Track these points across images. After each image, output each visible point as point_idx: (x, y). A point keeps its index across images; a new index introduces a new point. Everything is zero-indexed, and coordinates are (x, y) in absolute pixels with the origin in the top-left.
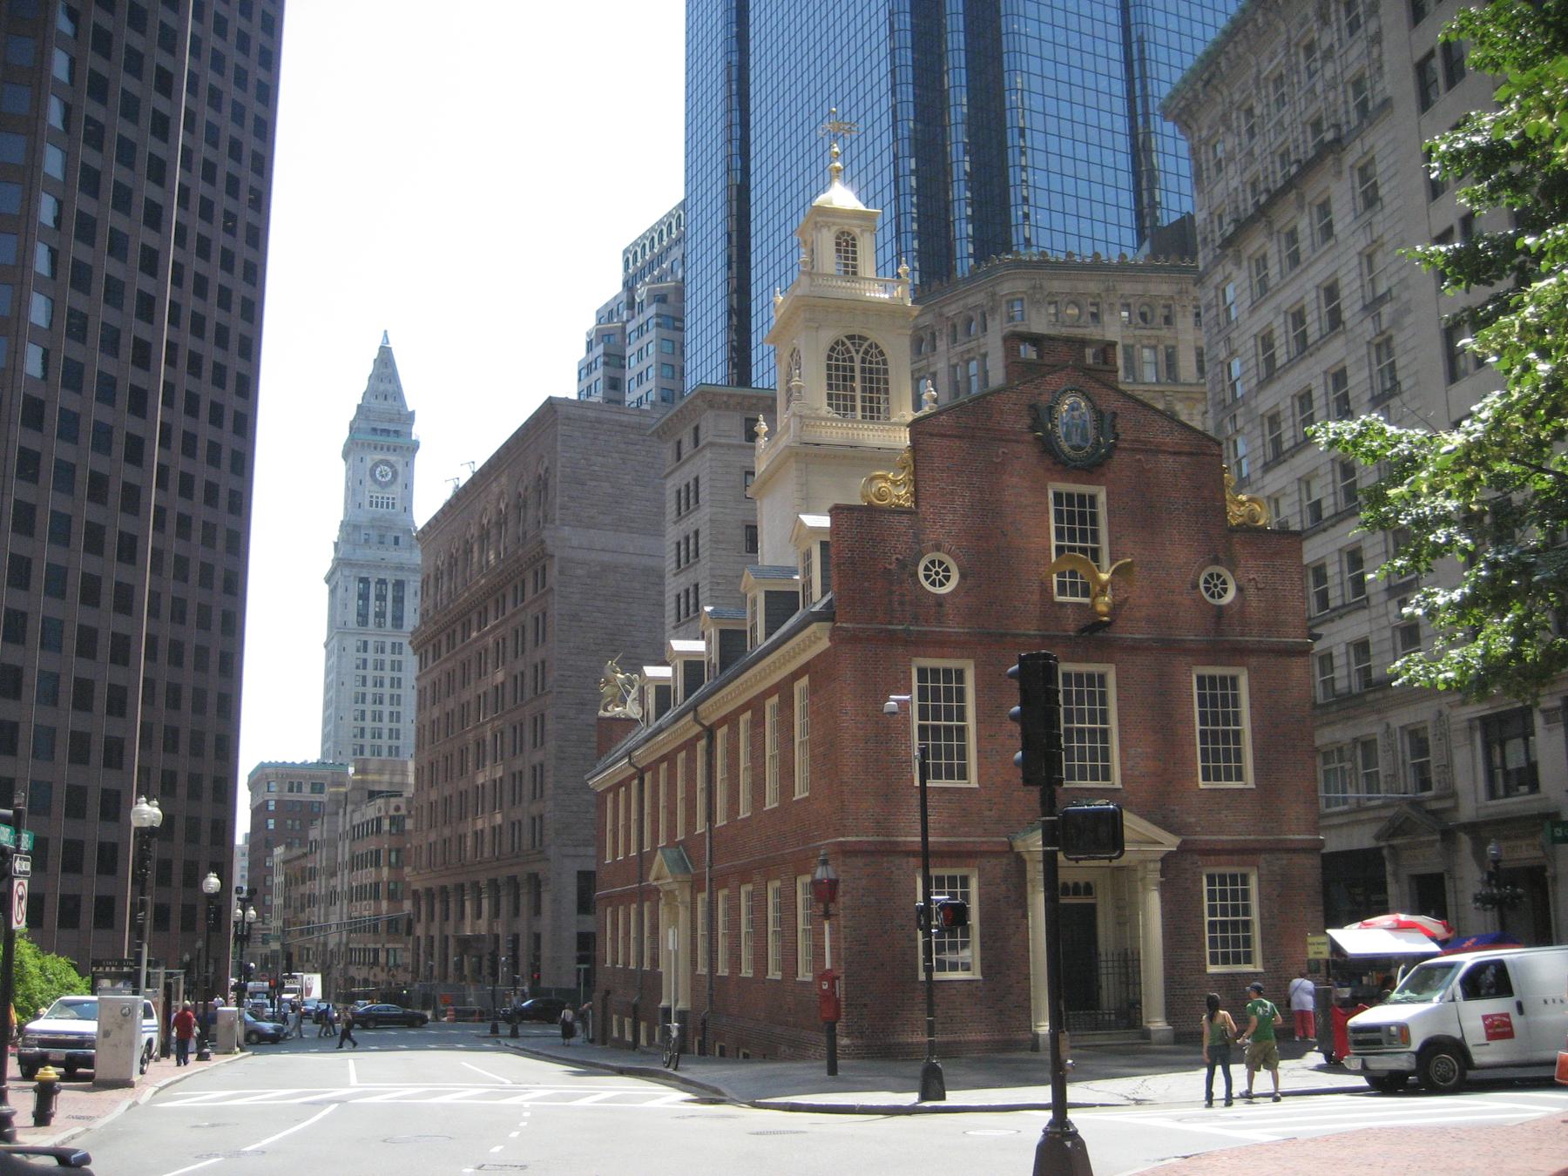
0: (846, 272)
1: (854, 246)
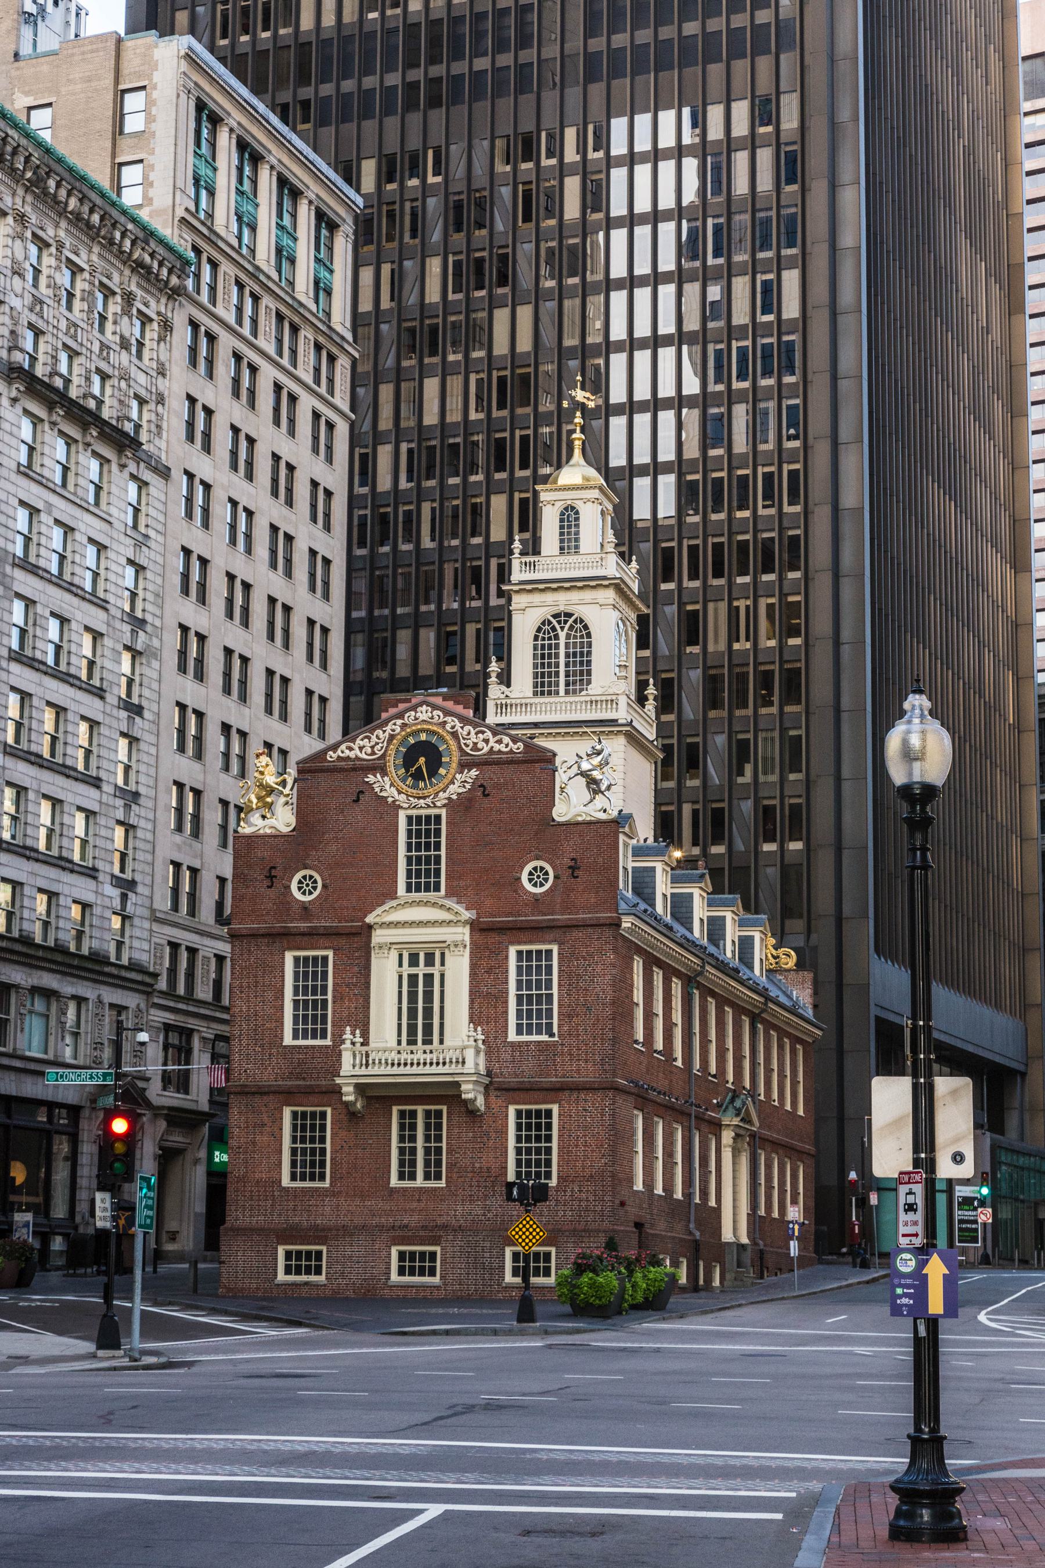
0: (562, 548)
1: (577, 519)
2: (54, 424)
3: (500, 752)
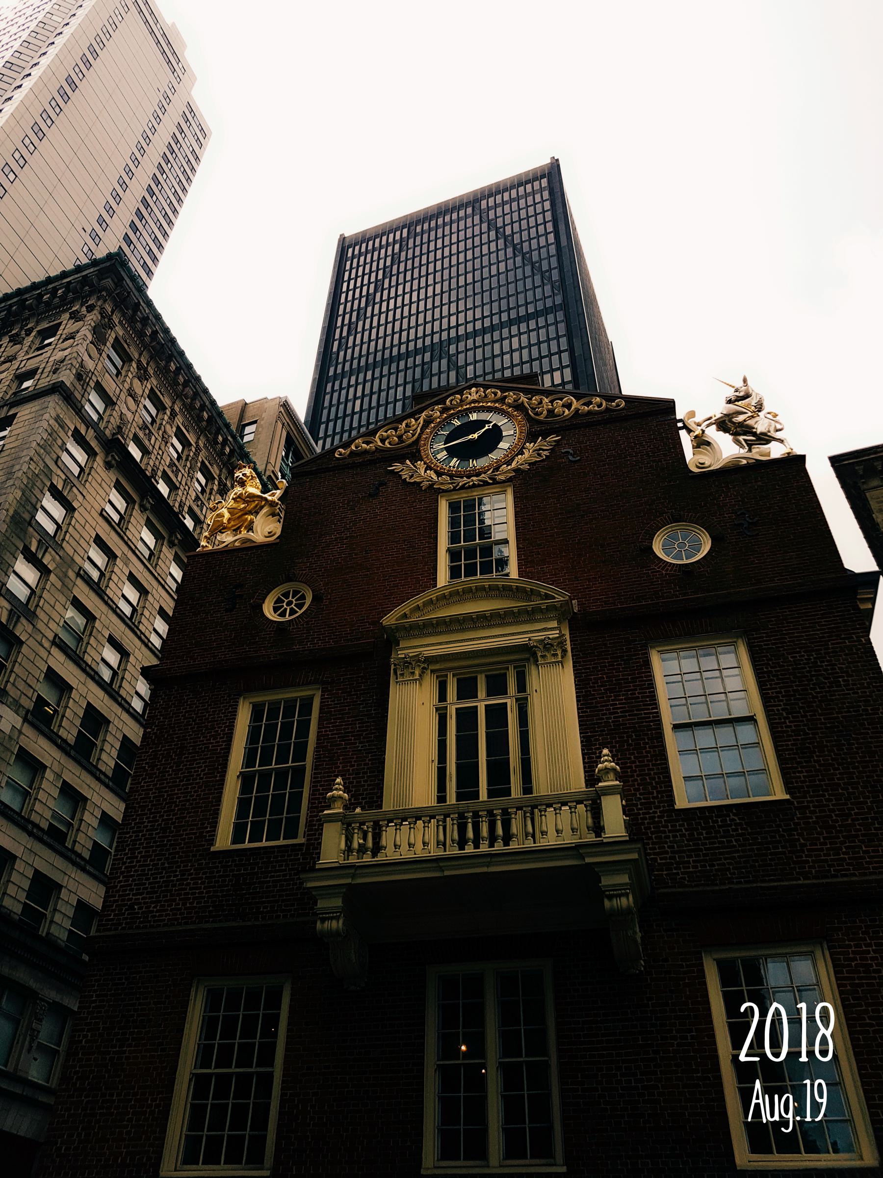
2: (143, 509)
3: (590, 413)
